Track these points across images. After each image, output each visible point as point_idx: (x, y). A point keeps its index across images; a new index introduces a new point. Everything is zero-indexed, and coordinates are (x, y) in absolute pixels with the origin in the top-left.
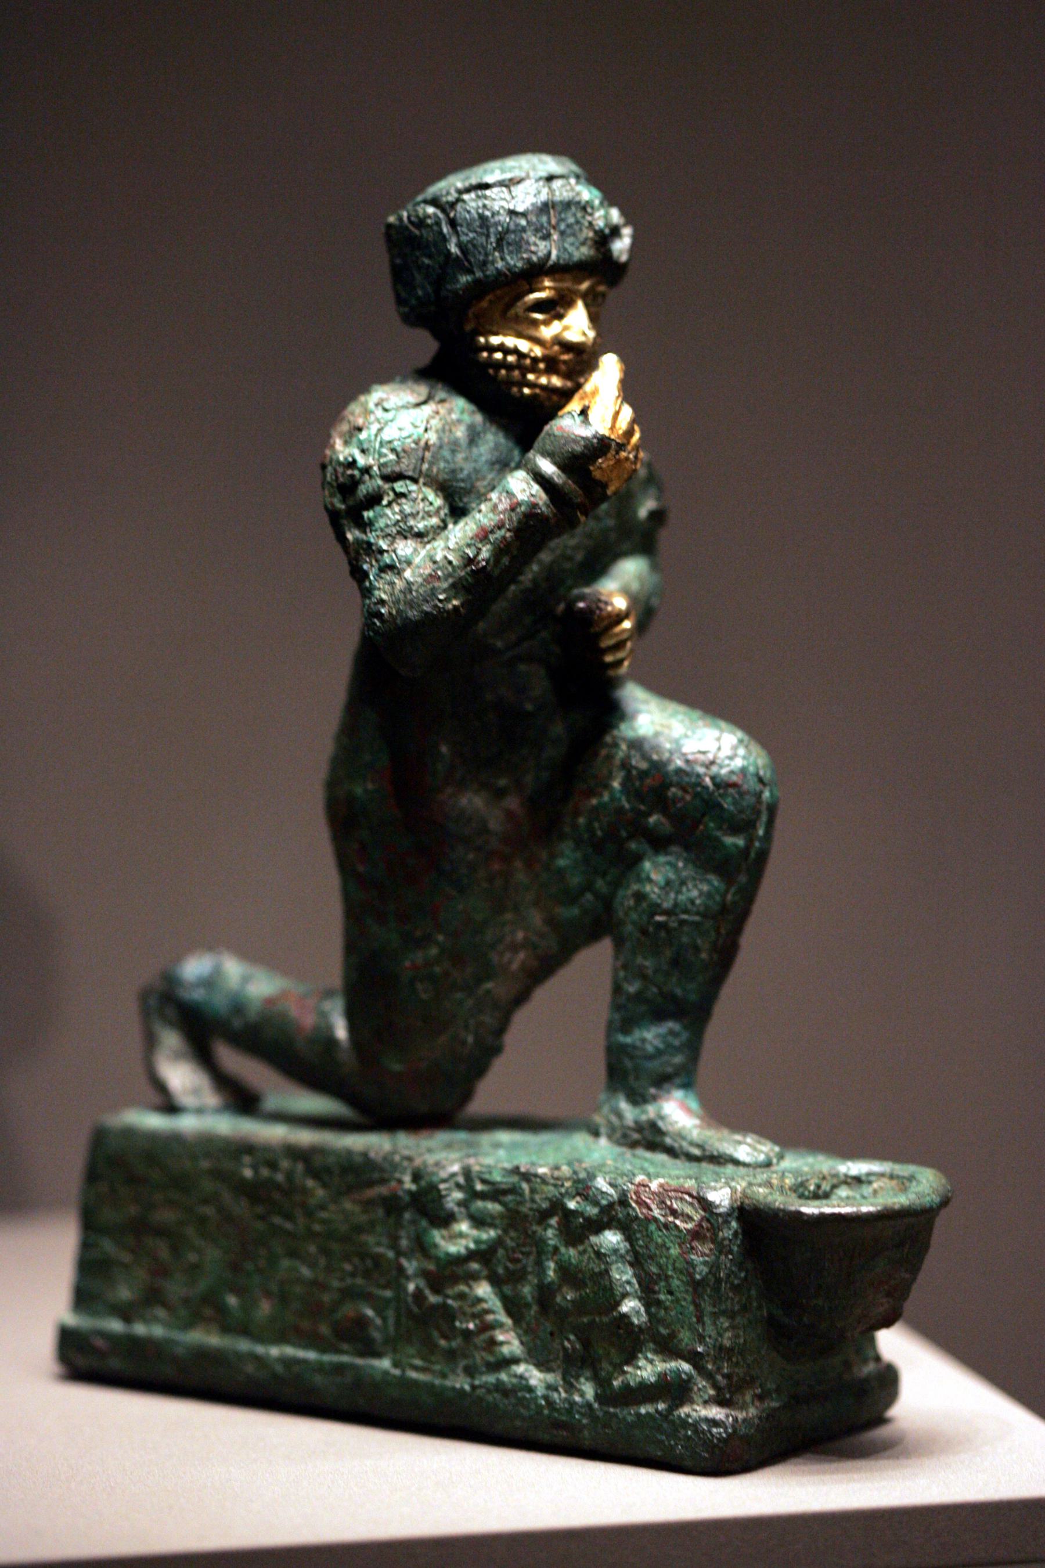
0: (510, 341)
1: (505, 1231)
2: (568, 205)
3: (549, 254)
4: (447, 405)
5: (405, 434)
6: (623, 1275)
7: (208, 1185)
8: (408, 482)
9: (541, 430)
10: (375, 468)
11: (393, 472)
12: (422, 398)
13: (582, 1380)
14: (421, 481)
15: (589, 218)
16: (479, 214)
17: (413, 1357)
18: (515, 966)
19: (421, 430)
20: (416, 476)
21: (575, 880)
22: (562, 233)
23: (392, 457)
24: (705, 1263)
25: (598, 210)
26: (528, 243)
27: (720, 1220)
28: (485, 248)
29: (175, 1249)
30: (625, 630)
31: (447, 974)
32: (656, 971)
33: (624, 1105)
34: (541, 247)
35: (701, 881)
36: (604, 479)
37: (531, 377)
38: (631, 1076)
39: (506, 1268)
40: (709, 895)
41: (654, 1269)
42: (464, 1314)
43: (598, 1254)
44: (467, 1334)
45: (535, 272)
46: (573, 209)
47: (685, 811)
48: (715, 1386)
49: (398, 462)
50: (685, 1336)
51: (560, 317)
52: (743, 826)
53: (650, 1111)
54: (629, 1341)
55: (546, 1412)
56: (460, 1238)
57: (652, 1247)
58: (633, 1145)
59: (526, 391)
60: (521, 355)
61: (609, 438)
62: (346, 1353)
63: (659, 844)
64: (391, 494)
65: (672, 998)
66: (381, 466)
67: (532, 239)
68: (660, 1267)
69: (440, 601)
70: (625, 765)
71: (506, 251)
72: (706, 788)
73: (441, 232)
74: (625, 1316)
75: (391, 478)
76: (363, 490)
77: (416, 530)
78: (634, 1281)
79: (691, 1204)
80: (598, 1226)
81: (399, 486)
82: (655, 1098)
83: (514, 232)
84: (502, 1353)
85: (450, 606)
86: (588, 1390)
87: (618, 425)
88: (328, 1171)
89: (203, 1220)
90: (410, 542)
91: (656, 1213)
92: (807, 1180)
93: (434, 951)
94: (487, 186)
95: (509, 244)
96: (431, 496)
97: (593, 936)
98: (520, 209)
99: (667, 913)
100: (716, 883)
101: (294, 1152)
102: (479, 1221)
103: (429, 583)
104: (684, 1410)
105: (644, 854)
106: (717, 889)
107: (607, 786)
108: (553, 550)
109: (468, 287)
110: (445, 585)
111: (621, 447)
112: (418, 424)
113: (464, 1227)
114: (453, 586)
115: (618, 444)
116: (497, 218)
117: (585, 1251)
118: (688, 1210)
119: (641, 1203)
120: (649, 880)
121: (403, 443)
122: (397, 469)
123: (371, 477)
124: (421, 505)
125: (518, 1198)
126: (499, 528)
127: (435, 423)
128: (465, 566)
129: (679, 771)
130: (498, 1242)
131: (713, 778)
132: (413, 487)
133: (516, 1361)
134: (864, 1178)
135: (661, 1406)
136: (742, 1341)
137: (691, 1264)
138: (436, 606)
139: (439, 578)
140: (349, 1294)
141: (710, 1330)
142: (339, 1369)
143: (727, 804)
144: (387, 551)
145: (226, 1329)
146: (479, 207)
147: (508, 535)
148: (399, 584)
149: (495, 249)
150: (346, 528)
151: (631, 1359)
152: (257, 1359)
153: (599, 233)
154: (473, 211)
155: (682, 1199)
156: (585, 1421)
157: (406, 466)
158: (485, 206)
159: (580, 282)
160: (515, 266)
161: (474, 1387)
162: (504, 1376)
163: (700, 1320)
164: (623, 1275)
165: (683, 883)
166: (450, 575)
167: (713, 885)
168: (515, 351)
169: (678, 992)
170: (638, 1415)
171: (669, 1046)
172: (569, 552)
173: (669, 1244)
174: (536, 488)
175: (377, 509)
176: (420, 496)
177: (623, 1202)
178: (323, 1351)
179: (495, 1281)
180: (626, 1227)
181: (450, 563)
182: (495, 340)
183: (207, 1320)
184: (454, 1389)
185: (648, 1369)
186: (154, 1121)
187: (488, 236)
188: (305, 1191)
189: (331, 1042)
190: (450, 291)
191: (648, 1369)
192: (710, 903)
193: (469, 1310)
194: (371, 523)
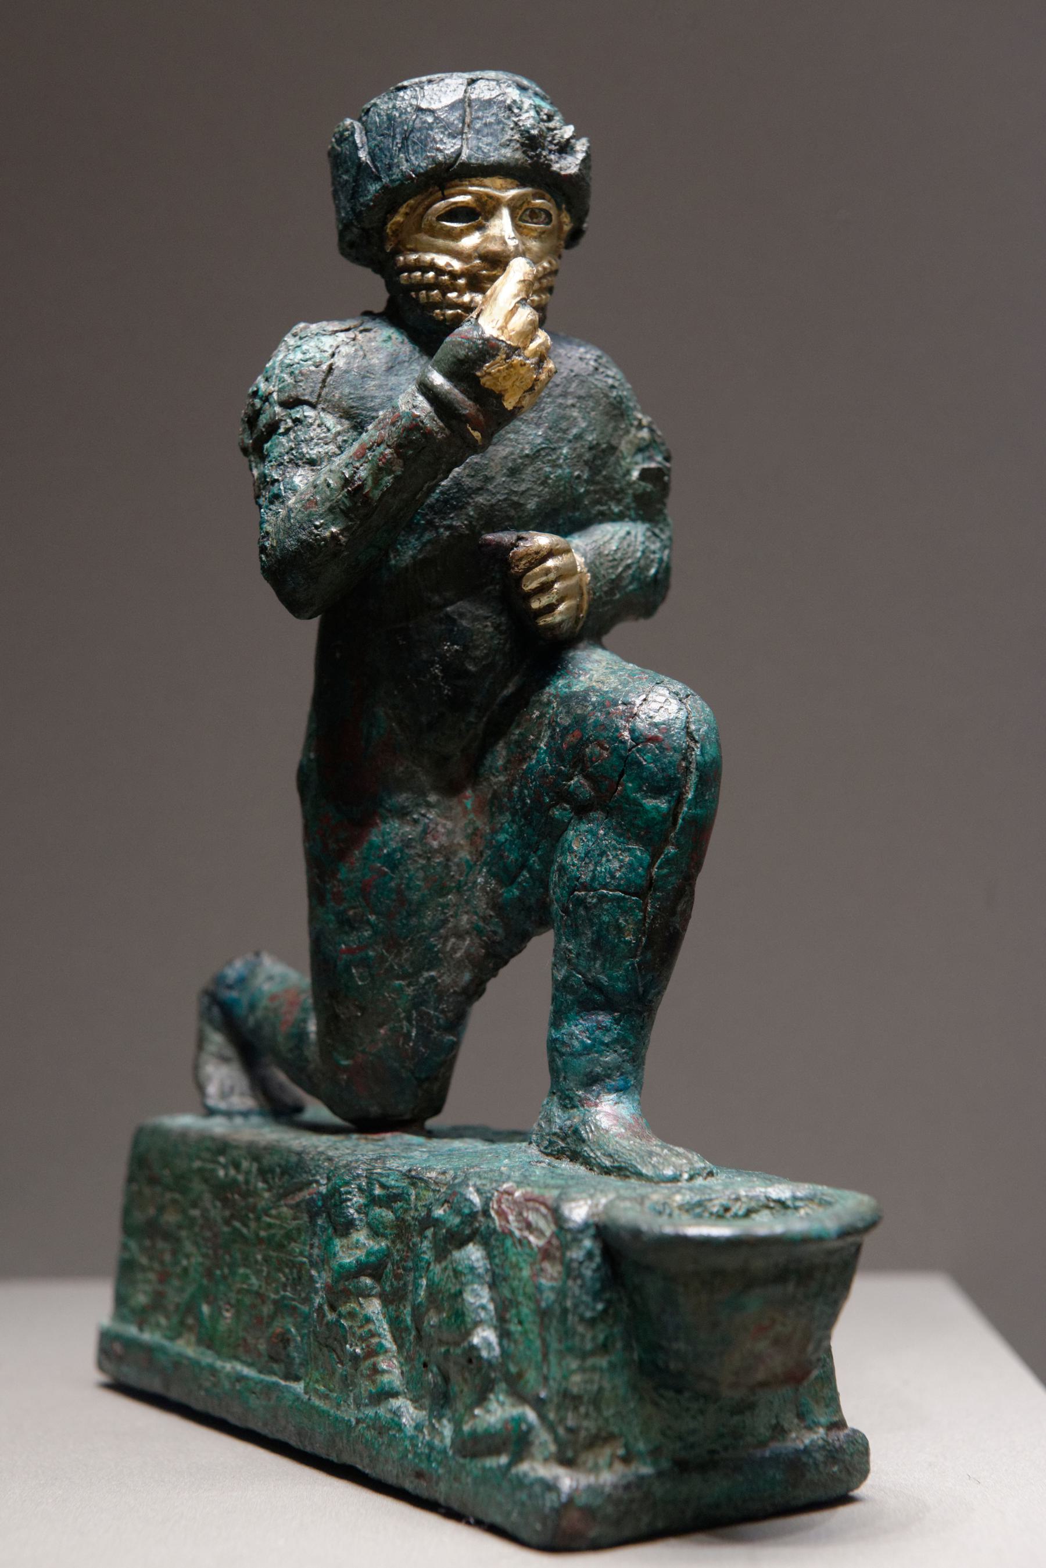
0: (428, 257)
1: (393, 1242)
2: (489, 103)
3: (459, 154)
5: (308, 356)
6: (479, 1297)
7: (197, 1186)
8: (306, 407)
9: (441, 342)
10: (275, 395)
11: (290, 397)
12: (344, 327)
13: (445, 1422)
14: (319, 406)
15: (516, 119)
16: (387, 115)
17: (317, 1381)
19: (327, 355)
21: (512, 857)
22: (478, 132)
23: (290, 380)
24: (552, 1288)
25: (527, 112)
27: (569, 1237)
28: (389, 150)
29: (174, 1253)
30: (548, 571)
31: (382, 959)
32: (578, 955)
33: (557, 1112)
34: (449, 147)
35: (624, 851)
37: (452, 295)
38: (572, 1079)
39: (392, 1285)
40: (631, 867)
41: (507, 1293)
42: (354, 1334)
43: (457, 1274)
44: (355, 1359)
46: (495, 110)
47: (613, 774)
48: (557, 1440)
49: (295, 387)
50: (531, 1376)
51: (480, 228)
52: (668, 785)
53: (577, 1115)
54: (484, 1378)
55: (410, 1456)
56: (358, 1246)
57: (507, 1265)
58: (559, 1155)
59: (450, 312)
60: (440, 271)
61: (497, 339)
62: (275, 1374)
63: (582, 810)
64: (289, 421)
65: (595, 986)
67: (439, 137)
68: (513, 1291)
69: (317, 527)
70: (552, 725)
71: (411, 151)
72: (624, 742)
73: (354, 142)
74: (473, 1348)
75: (291, 403)
76: (263, 420)
77: (308, 456)
78: (491, 1307)
79: (544, 1216)
80: (458, 1239)
81: (297, 413)
82: (582, 1102)
83: (420, 130)
84: (382, 1382)
85: (327, 534)
86: (447, 1430)
87: (510, 326)
88: (272, 1171)
89: (192, 1221)
91: (514, 1225)
92: (711, 1200)
94: (405, 88)
95: (415, 143)
96: (330, 420)
97: (544, 923)
98: (424, 105)
99: (584, 887)
100: (639, 853)
101: (255, 1153)
102: (375, 1232)
103: (306, 509)
104: (524, 1467)
105: (569, 822)
106: (640, 861)
107: (536, 748)
109: (376, 198)
110: (321, 510)
111: (513, 350)
112: (326, 348)
113: (361, 1236)
114: (331, 510)
115: (509, 346)
116: (404, 117)
117: (446, 1268)
118: (542, 1224)
119: (501, 1214)
120: (571, 851)
121: (302, 366)
122: (293, 394)
123: (270, 404)
124: (319, 430)
125: (405, 1206)
126: (379, 445)
128: (344, 487)
129: (597, 725)
130: (387, 1254)
131: (632, 731)
132: (309, 412)
133: (395, 1395)
134: (789, 1203)
135: (504, 1460)
136: (595, 1387)
137: (539, 1288)
138: (311, 533)
139: (316, 503)
140: (281, 1307)
141: (555, 1372)
142: (269, 1389)
143: (645, 760)
144: (277, 481)
145: (200, 1342)
146: (388, 109)
147: (388, 451)
148: (283, 512)
149: (400, 149)
150: (253, 464)
151: (481, 1399)
152: (213, 1371)
153: (525, 133)
154: (382, 113)
155: (537, 1210)
156: (441, 1471)
157: (305, 391)
158: (394, 107)
159: (507, 189)
160: (419, 165)
161: (358, 1421)
162: (382, 1411)
164: (479, 1297)
165: (603, 853)
166: (328, 499)
167: (635, 857)
169: (603, 979)
170: (484, 1469)
173: (523, 1265)
174: (421, 400)
175: (274, 437)
176: (317, 422)
177: (486, 1213)
178: (260, 1372)
179: (386, 1300)
180: (489, 1239)
181: (329, 485)
183: (190, 1329)
184: (343, 1419)
185: (497, 1412)
186: (185, 1121)
187: (394, 137)
188: (255, 1193)
189: (301, 1036)
190: (362, 205)
191: (497, 1412)
192: (632, 875)
193: (359, 1332)
194: (268, 455)
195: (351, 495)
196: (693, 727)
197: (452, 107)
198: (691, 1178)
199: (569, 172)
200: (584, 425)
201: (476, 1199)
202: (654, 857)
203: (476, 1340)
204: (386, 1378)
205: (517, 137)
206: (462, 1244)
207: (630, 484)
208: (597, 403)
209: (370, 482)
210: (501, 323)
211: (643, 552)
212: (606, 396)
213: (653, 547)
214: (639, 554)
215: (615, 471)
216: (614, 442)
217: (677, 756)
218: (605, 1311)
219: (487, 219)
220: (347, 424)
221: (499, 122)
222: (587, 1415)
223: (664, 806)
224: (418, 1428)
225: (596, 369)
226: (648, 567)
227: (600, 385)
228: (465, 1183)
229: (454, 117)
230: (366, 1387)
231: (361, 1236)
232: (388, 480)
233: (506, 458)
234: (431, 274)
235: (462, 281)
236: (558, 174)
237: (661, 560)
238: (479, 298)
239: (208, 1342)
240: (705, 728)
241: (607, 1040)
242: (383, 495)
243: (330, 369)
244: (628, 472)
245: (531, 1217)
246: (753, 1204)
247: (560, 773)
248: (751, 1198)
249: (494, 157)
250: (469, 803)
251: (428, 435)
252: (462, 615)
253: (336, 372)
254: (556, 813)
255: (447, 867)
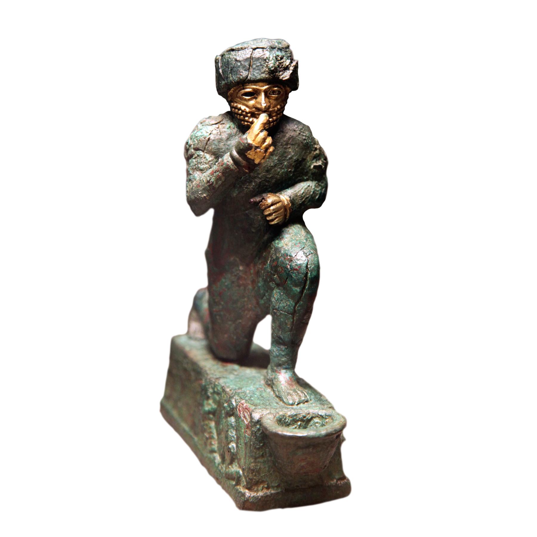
0: (239, 106)
2: (258, 59)
3: (247, 77)
4: (224, 125)
5: (202, 134)
18: (248, 316)
20: (203, 149)
23: (197, 142)
26: (240, 72)
34: (244, 74)
36: (252, 158)
37: (247, 118)
45: (244, 82)
46: (260, 61)
51: (256, 98)
59: (246, 123)
66: (194, 145)
67: (241, 70)
72: (288, 269)
75: (197, 149)
76: (189, 153)
87: (256, 140)
90: (198, 172)
91: (242, 415)
93: (221, 307)
98: (238, 59)
99: (276, 309)
106: (292, 305)
108: (260, 178)
111: (257, 147)
114: (204, 189)
118: (247, 417)
127: (215, 132)
132: (201, 153)
157: (200, 146)
163: (245, 456)
165: (281, 301)
166: (202, 186)
168: (240, 109)
171: (280, 354)
172: (268, 179)
182: (235, 105)
195: (209, 186)
196: (309, 266)
197: (247, 60)
198: (298, 404)
199: (286, 78)
200: (293, 154)
201: (234, 404)
202: (296, 304)
203: (230, 446)
204: (213, 447)
205: (267, 70)
206: (230, 416)
207: (310, 170)
208: (299, 145)
209: (215, 183)
210: (253, 139)
211: (314, 192)
212: (302, 143)
213: (318, 189)
214: (312, 193)
215: (305, 166)
216: (304, 158)
217: (303, 276)
218: (263, 446)
219: (257, 95)
220: (213, 157)
221: (261, 65)
222: (255, 475)
223: (299, 290)
224: (219, 464)
225: (300, 134)
226: (315, 196)
227: (300, 139)
228: (232, 397)
229: (247, 64)
230: (209, 448)
231: (211, 402)
232: (220, 182)
233: (265, 167)
234: (240, 111)
235: (249, 115)
236: (282, 80)
237: (321, 193)
238: (255, 120)
239: (181, 415)
240: (313, 266)
241: (283, 354)
242: (219, 186)
243: (209, 139)
244: (310, 166)
245: (246, 414)
246: (314, 415)
247: (271, 273)
248: (313, 414)
249: (259, 77)
250: (252, 271)
251: (232, 170)
252: (251, 214)
253: (211, 141)
254: (271, 284)
255: (245, 290)
